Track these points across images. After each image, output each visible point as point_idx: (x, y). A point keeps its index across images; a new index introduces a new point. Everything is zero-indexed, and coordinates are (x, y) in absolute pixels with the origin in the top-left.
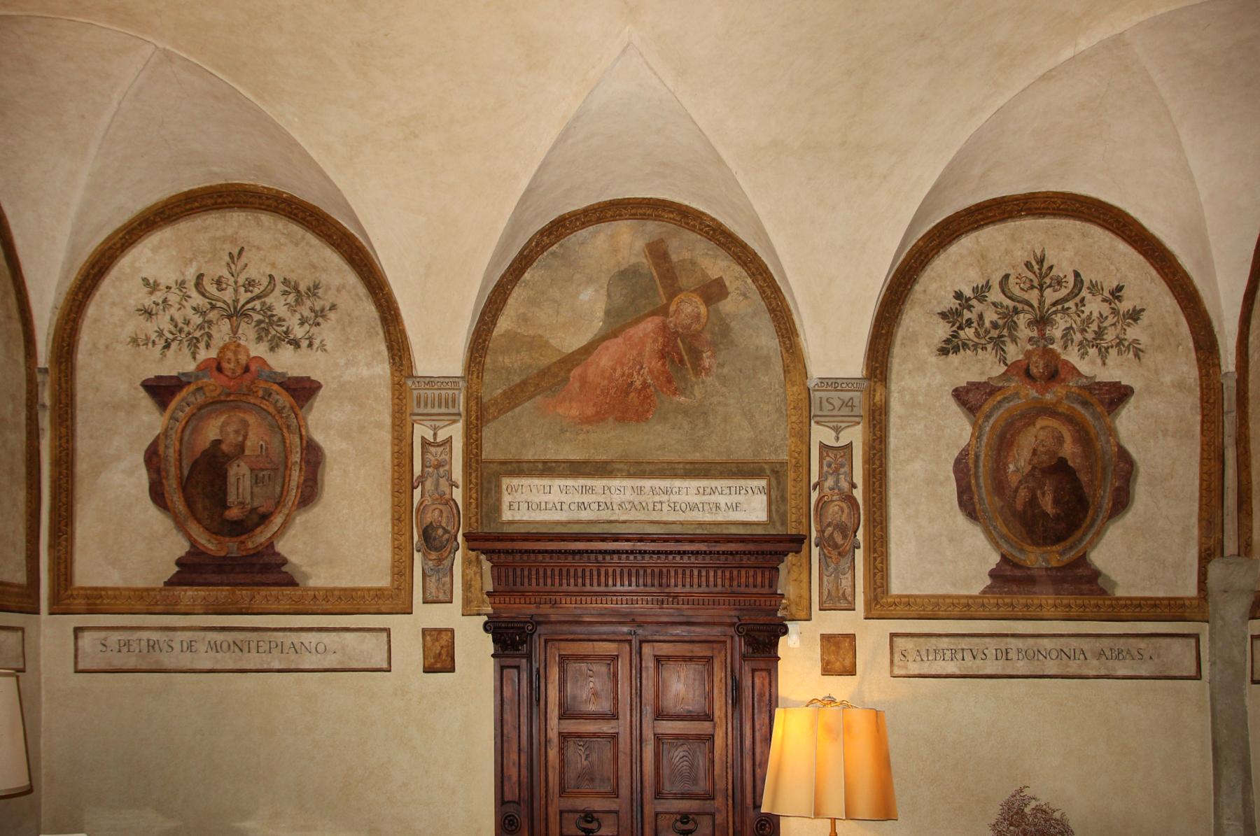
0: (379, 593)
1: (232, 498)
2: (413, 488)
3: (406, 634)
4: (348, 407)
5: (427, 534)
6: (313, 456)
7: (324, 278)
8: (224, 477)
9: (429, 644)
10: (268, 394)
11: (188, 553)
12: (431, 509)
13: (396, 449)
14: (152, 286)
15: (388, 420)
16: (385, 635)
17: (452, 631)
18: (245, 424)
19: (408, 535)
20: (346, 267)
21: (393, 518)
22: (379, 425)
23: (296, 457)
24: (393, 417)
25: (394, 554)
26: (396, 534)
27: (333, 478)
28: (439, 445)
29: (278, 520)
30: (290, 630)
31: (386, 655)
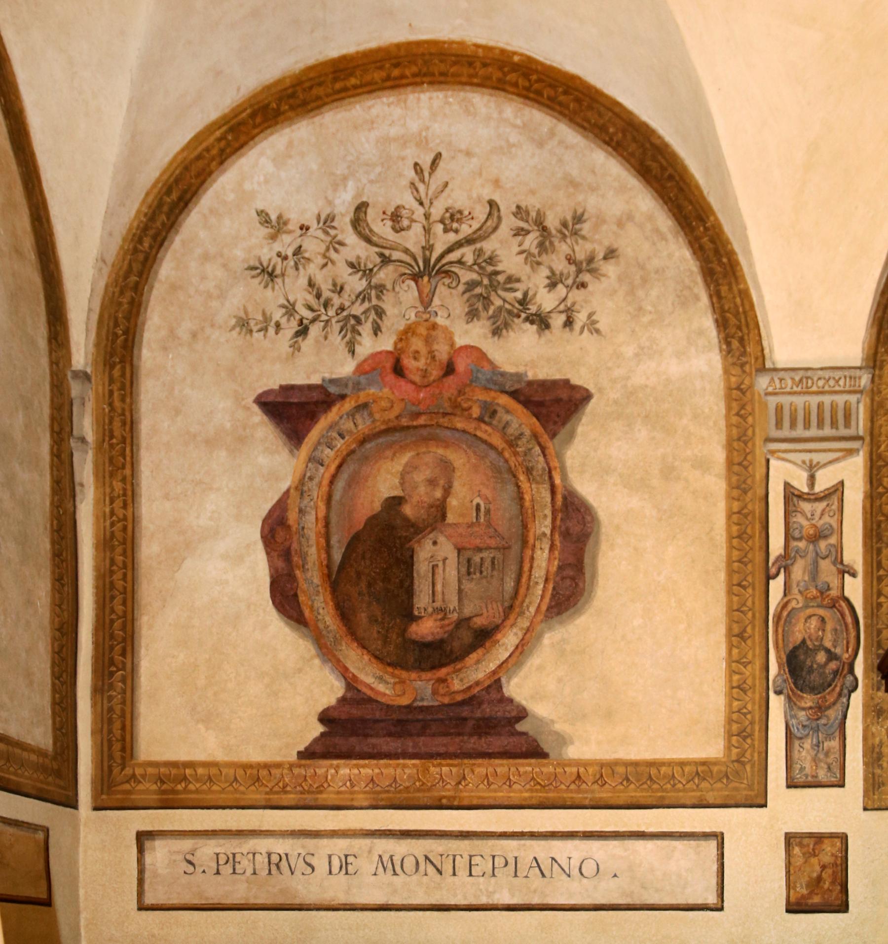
0: (702, 770)
1: (422, 601)
2: (768, 578)
3: (755, 841)
4: (642, 433)
5: (795, 662)
6: (576, 524)
7: (591, 203)
8: (408, 563)
9: (798, 861)
10: (490, 413)
11: (342, 700)
12: (803, 615)
13: (736, 506)
14: (275, 225)
15: (720, 456)
16: (713, 844)
17: (843, 838)
18: (447, 467)
19: (758, 664)
20: (633, 182)
21: (730, 634)
22: (702, 464)
23: (543, 525)
24: (729, 447)
25: (731, 698)
26: (736, 663)
27: (614, 564)
28: (818, 499)
29: (509, 639)
30: (533, 835)
31: (714, 881)
